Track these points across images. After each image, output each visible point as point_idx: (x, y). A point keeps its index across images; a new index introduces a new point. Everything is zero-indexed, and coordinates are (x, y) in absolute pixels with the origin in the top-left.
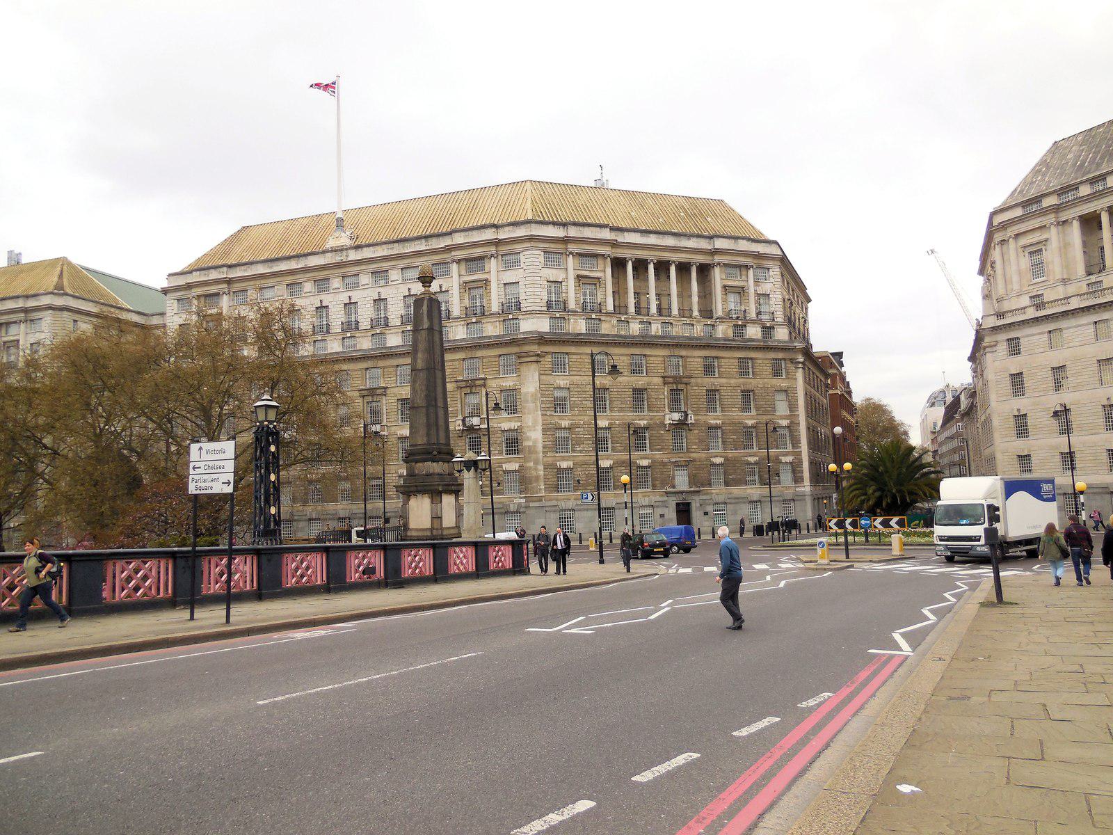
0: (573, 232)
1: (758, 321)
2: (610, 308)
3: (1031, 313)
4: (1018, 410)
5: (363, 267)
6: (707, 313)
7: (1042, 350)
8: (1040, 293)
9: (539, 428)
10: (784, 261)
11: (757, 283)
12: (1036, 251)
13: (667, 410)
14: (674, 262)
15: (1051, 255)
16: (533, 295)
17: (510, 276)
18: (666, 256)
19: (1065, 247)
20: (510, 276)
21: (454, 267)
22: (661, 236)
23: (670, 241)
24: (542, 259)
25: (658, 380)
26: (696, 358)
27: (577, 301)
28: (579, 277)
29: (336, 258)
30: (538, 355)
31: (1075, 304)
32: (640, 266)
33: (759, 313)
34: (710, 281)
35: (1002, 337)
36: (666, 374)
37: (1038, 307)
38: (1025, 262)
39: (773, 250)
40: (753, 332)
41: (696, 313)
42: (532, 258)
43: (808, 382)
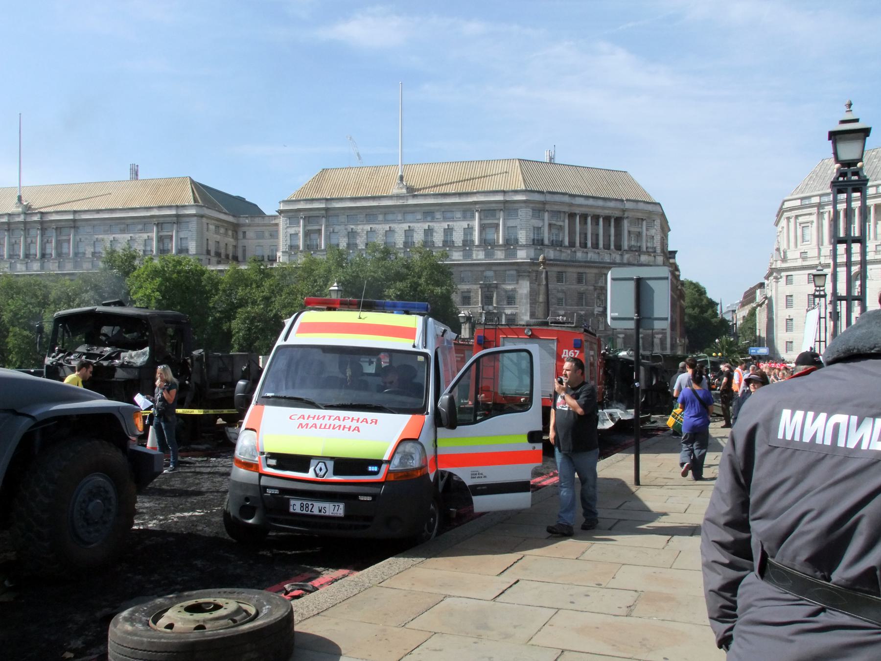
0: (549, 198)
2: (566, 243)
3: (799, 263)
4: (789, 316)
5: (418, 208)
6: (618, 247)
7: (804, 284)
8: (806, 251)
9: (529, 314)
10: (663, 215)
11: (647, 230)
13: (595, 305)
14: (602, 216)
17: (511, 223)
18: (598, 212)
20: (511, 223)
22: (595, 200)
24: (531, 214)
25: (591, 288)
27: (549, 240)
28: (550, 225)
29: (400, 202)
30: (529, 272)
33: (647, 248)
34: (621, 227)
35: (784, 274)
36: (595, 285)
37: (804, 259)
39: (657, 208)
41: (612, 247)
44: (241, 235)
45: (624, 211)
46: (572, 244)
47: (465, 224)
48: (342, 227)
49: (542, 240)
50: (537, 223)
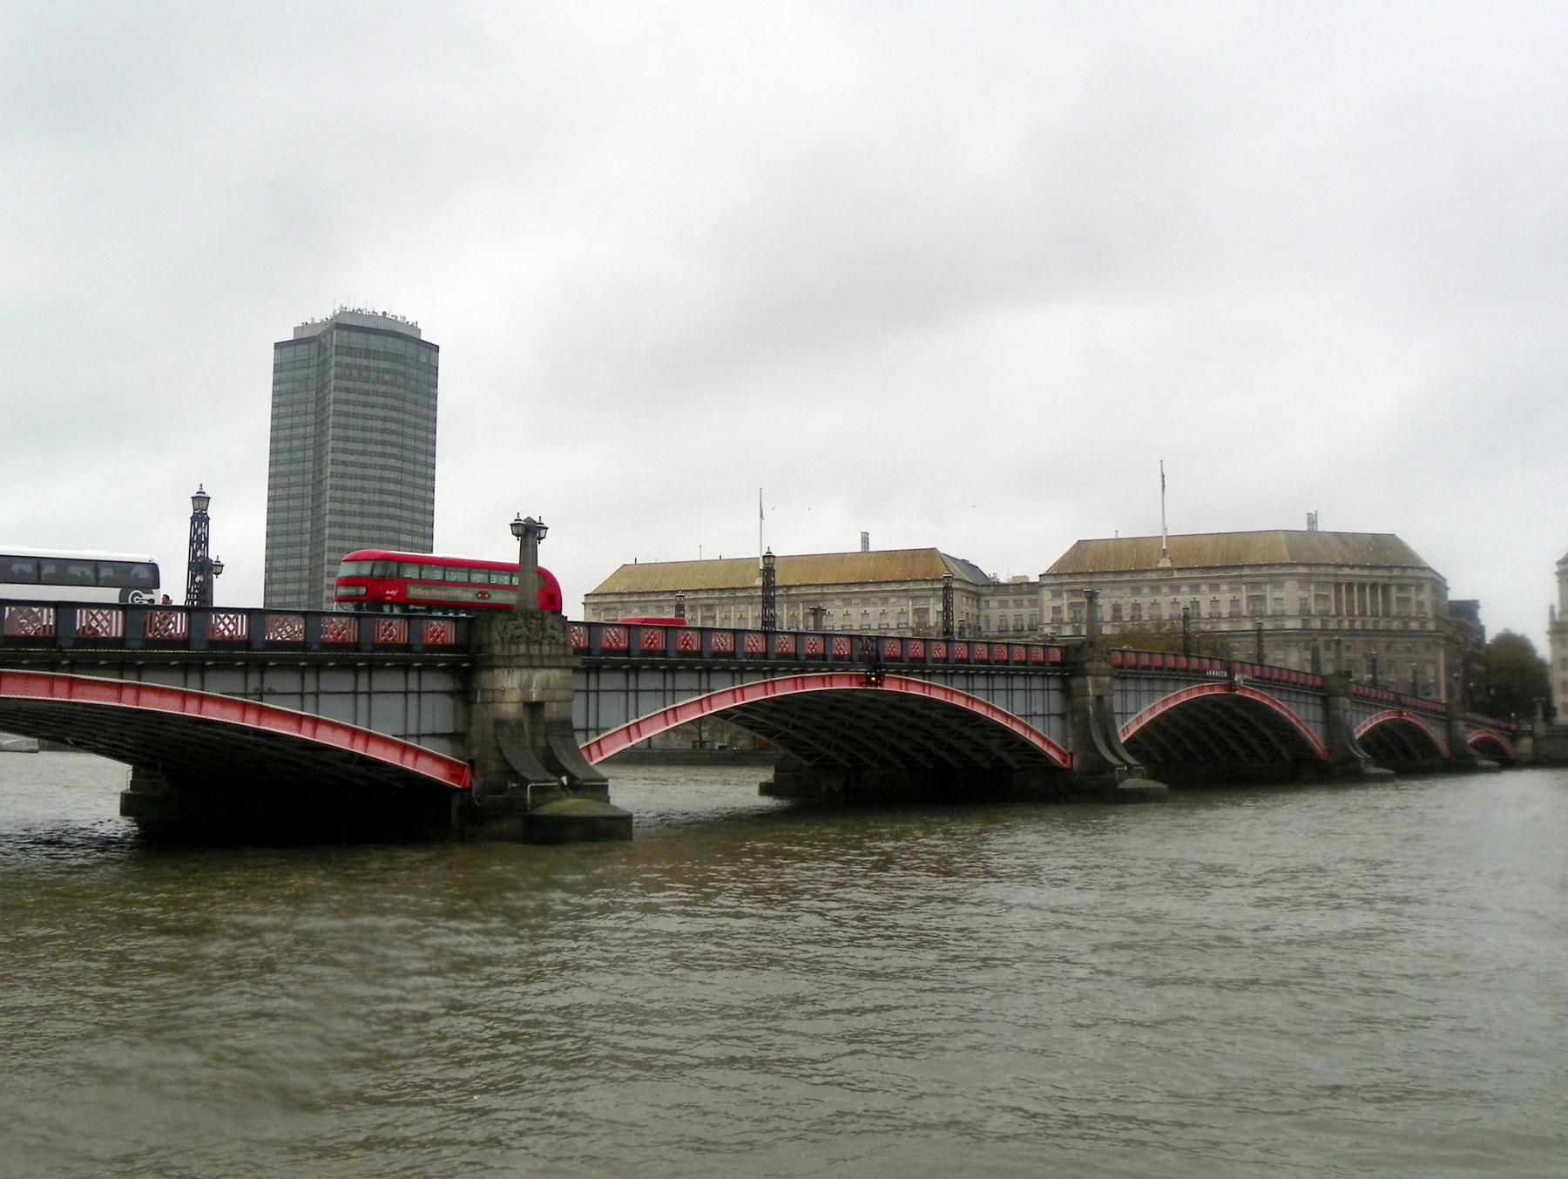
1: (1417, 619)
2: (1333, 612)
6: (1387, 613)
16: (1291, 607)
17: (1278, 594)
18: (1364, 580)
20: (1278, 594)
21: (1244, 587)
26: (1381, 642)
28: (1316, 596)
32: (1350, 586)
40: (1414, 625)
43: (1447, 654)
44: (983, 604)
45: (1390, 577)
46: (1339, 613)
47: (1230, 596)
48: (1106, 600)
49: (1309, 611)
50: (1304, 594)
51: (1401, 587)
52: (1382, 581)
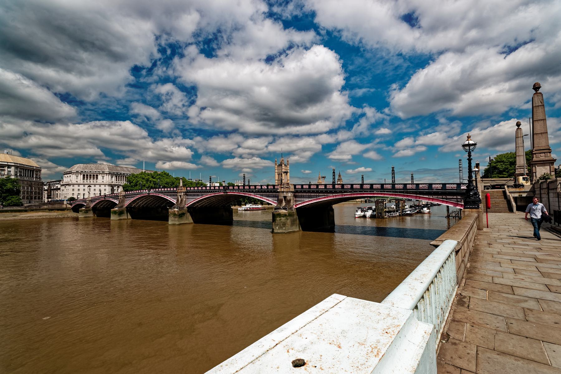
3: (76, 183)
12: (77, 176)
15: (79, 177)
17: (9, 170)
19: (80, 177)
23: (29, 167)
31: (81, 183)
38: (76, 177)
42: (13, 168)
51: (37, 171)
52: (32, 169)
